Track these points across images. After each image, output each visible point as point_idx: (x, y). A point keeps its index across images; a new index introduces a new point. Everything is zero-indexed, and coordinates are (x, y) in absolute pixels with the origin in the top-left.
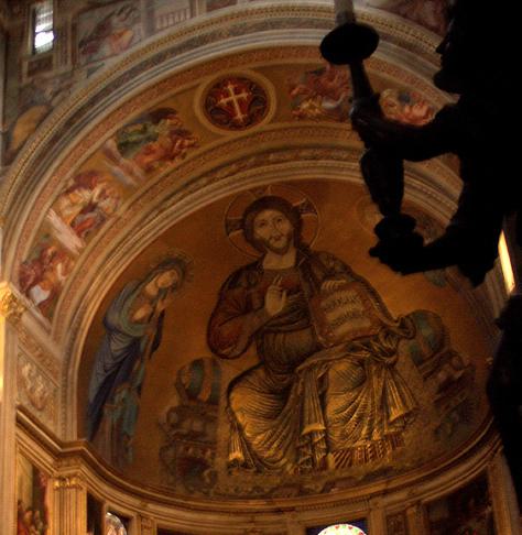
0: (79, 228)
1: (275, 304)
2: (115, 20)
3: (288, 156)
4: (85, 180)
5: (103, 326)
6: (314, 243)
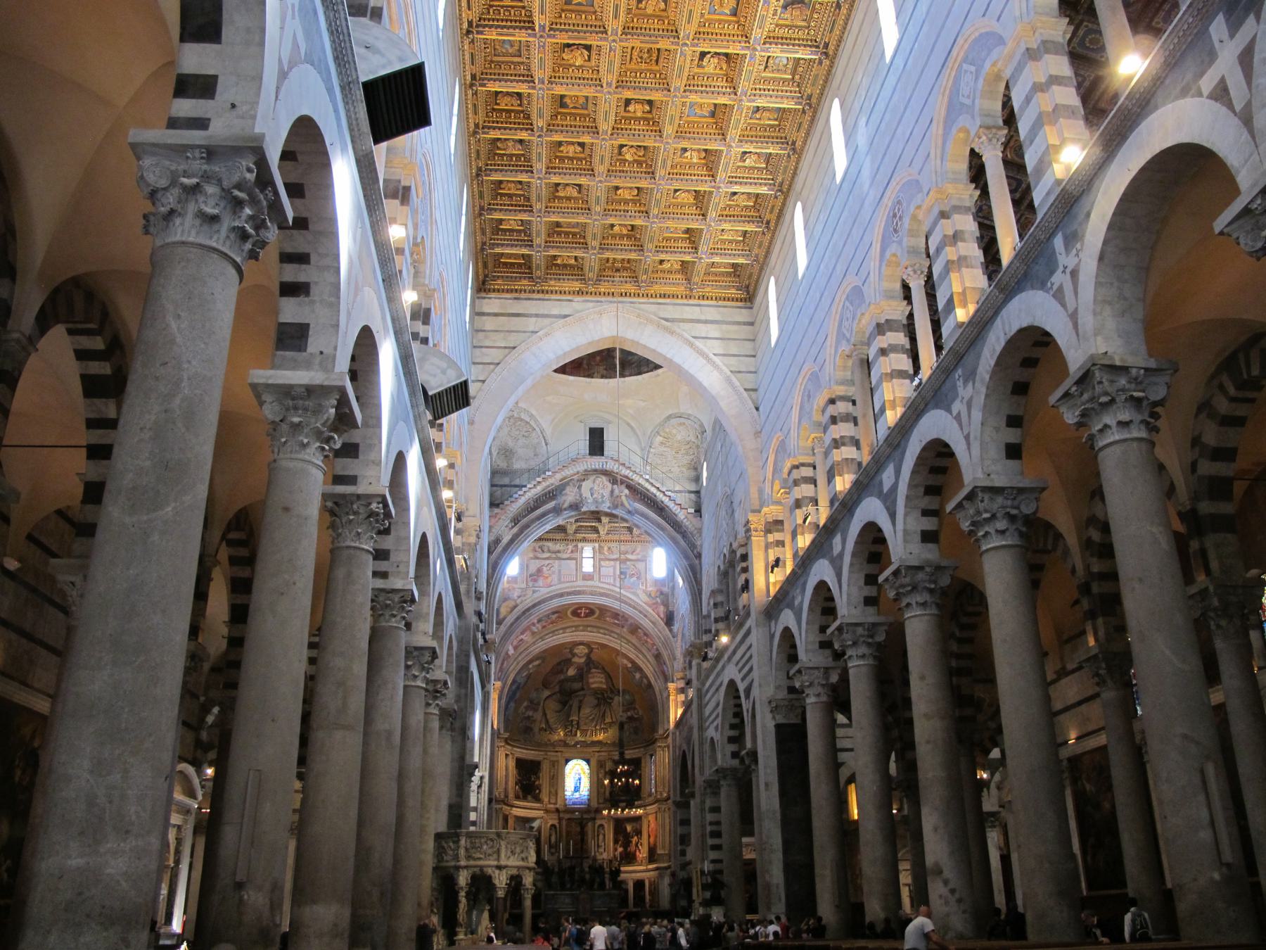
0: (515, 648)
1: (571, 672)
2: (545, 568)
3: (595, 630)
4: (522, 634)
5: (514, 681)
6: (593, 657)
